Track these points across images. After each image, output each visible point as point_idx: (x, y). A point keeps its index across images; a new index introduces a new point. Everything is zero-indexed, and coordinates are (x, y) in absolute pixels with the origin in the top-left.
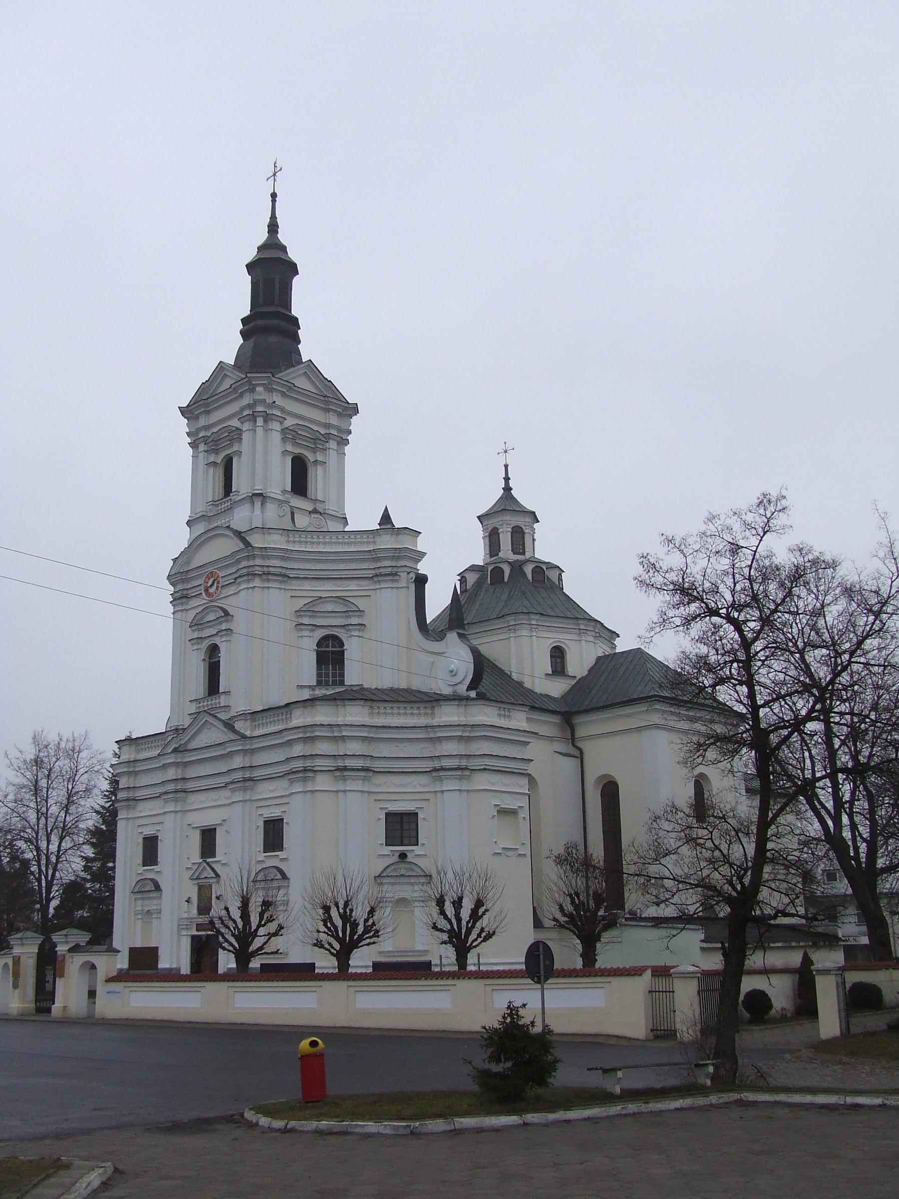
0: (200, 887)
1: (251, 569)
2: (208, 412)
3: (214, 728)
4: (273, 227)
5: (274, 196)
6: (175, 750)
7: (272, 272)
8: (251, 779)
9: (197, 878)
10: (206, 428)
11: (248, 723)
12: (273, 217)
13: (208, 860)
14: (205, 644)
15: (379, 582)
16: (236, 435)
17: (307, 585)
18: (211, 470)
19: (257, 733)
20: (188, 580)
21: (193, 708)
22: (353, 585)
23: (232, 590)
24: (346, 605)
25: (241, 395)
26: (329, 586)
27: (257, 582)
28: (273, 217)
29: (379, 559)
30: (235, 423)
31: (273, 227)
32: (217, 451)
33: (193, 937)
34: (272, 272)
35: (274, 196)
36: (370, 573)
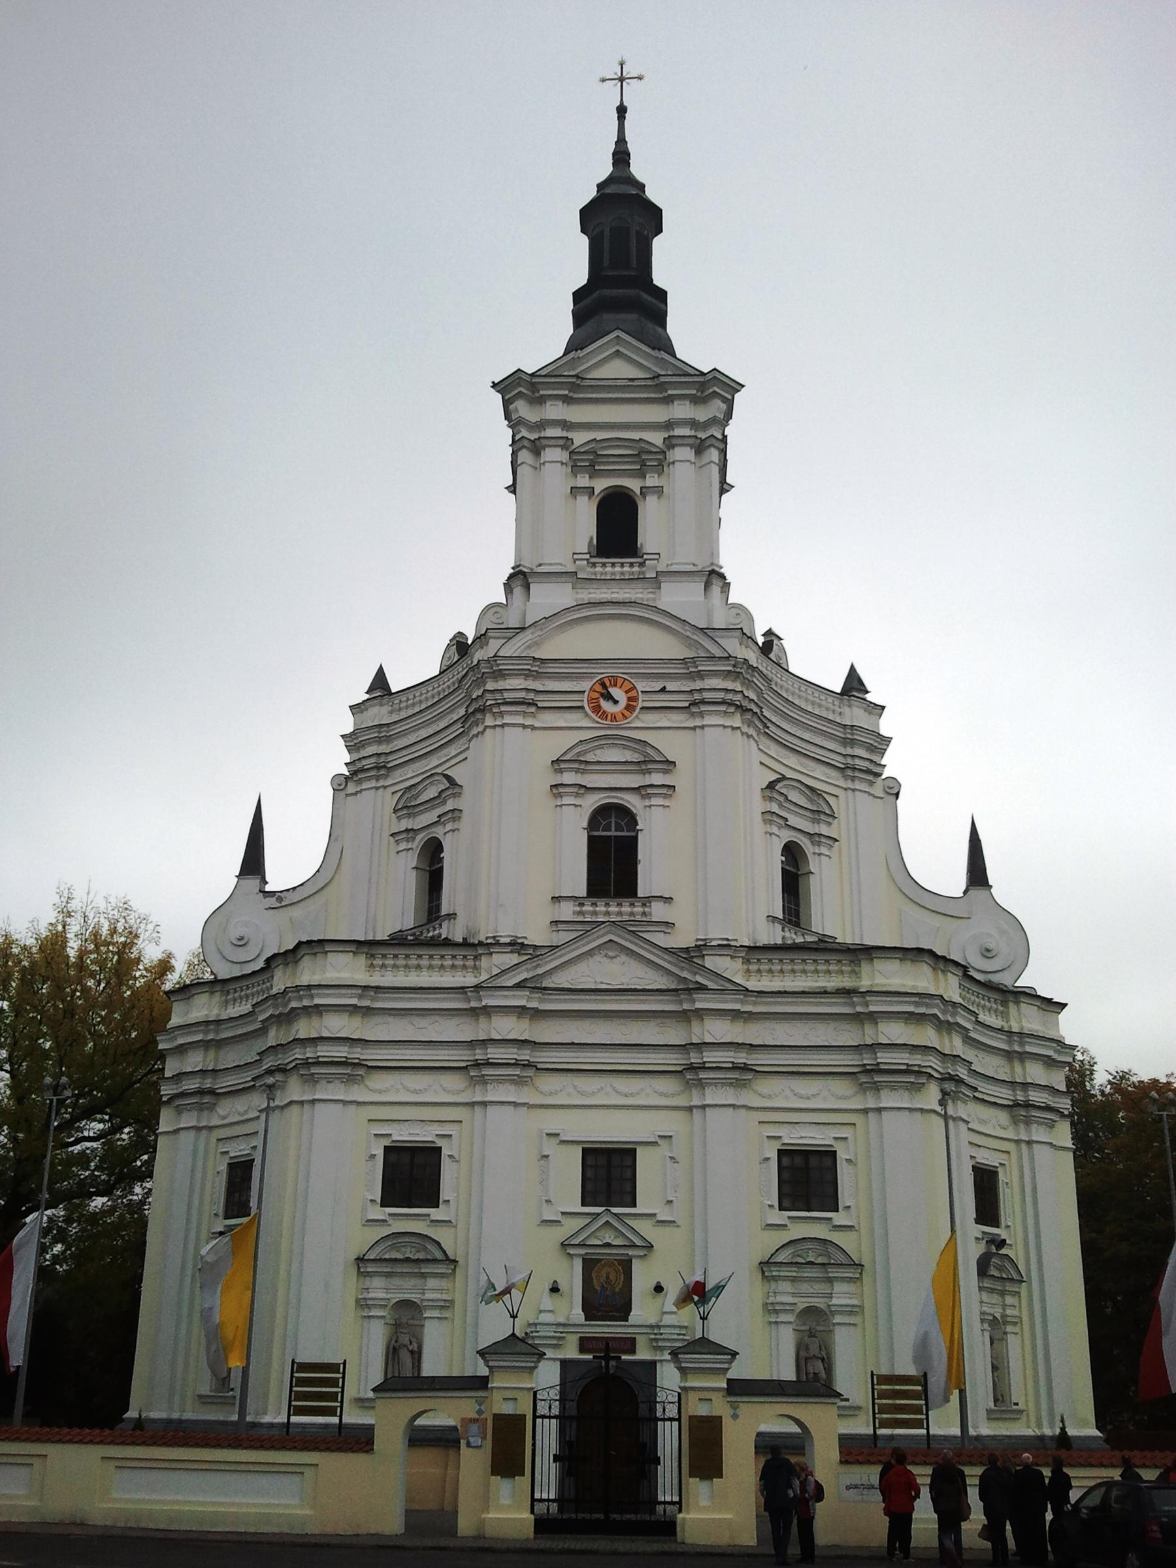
0: (589, 1265)
1: (730, 696)
2: (567, 400)
3: (623, 958)
4: (621, 156)
5: (622, 111)
6: (519, 986)
7: (621, 222)
8: (745, 1068)
9: (582, 1245)
10: (565, 425)
11: (738, 964)
12: (621, 141)
13: (615, 1210)
14: (592, 802)
15: (853, 779)
16: (649, 460)
17: (774, 750)
18: (583, 500)
19: (753, 984)
20: (537, 676)
21: (567, 911)
22: (819, 771)
23: (663, 720)
24: (811, 801)
25: (669, 400)
26: (792, 760)
27: (737, 721)
28: (621, 141)
29: (852, 743)
30: (657, 438)
31: (621, 156)
32: (594, 473)
33: (564, 1363)
34: (621, 222)
35: (622, 111)
36: (838, 760)
